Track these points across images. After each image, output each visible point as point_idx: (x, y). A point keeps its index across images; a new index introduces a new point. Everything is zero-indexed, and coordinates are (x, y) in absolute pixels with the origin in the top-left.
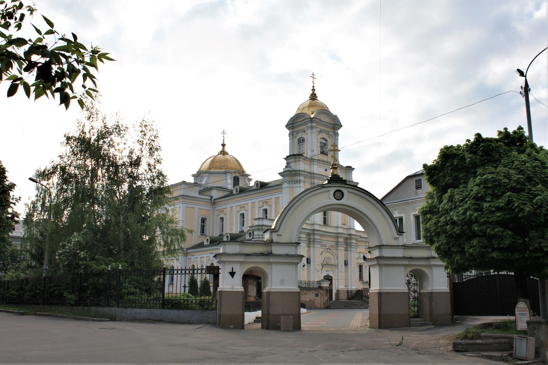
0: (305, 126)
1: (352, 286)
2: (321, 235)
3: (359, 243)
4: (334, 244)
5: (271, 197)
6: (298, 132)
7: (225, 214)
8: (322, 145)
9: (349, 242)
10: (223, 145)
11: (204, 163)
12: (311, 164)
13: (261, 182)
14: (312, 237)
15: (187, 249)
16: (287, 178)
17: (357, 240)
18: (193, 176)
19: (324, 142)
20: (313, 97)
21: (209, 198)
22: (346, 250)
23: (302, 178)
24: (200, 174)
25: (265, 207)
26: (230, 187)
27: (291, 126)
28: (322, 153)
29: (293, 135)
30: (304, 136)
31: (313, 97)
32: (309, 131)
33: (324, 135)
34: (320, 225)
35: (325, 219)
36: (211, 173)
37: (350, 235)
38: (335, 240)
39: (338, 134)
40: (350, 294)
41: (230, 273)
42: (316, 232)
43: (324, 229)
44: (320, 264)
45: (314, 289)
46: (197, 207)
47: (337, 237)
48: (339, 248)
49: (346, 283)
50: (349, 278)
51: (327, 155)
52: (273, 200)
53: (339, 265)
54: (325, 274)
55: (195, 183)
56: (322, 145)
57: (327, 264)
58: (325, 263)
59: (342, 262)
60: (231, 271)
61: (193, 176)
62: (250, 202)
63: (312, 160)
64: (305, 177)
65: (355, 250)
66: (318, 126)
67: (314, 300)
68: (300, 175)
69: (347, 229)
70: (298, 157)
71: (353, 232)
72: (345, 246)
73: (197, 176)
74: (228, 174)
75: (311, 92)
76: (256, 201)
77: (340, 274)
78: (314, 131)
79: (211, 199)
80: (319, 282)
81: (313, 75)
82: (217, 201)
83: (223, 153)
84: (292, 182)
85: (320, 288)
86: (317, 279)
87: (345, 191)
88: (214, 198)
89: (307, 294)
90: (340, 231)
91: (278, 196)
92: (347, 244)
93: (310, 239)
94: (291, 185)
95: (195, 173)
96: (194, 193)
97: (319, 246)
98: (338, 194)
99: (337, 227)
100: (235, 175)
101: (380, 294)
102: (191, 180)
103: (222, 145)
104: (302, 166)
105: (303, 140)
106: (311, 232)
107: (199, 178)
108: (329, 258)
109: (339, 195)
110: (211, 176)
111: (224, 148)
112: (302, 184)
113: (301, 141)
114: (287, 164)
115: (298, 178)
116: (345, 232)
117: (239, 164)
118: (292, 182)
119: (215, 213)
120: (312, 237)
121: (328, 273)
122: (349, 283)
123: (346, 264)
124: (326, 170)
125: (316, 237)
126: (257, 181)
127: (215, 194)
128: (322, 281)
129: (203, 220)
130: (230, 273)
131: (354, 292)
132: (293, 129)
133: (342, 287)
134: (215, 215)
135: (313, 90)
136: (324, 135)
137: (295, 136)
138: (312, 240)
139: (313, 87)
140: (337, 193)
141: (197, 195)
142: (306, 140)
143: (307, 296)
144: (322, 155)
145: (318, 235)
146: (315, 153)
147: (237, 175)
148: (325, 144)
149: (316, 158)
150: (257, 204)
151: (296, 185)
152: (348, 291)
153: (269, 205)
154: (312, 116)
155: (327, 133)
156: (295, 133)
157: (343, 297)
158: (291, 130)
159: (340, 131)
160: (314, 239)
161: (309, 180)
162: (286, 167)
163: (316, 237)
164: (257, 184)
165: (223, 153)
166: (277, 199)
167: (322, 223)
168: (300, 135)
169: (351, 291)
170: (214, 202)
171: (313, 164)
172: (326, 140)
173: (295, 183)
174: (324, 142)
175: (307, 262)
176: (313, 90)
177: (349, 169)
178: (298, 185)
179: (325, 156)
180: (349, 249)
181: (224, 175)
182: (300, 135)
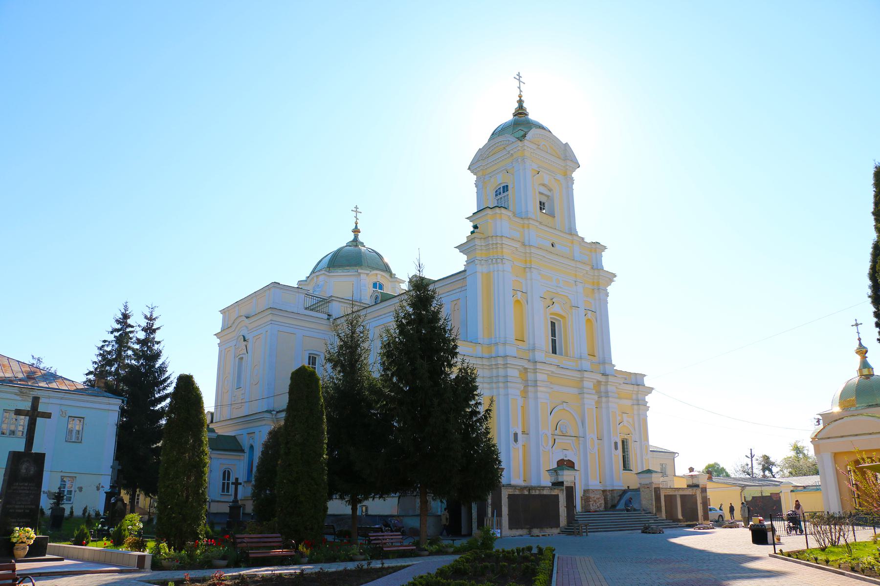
10: (356, 231)
11: (320, 261)
14: (531, 376)
35: (554, 342)
40: (609, 497)
43: (554, 359)
58: (557, 432)
75: (516, 105)
79: (328, 319)
82: (338, 322)
83: (356, 242)
92: (598, 392)
100: (375, 280)
105: (506, 188)
114: (475, 227)
120: (531, 376)
133: (595, 484)
135: (520, 102)
138: (530, 383)
157: (598, 503)
159: (575, 175)
162: (472, 233)
165: (356, 242)
168: (500, 179)
176: (520, 102)
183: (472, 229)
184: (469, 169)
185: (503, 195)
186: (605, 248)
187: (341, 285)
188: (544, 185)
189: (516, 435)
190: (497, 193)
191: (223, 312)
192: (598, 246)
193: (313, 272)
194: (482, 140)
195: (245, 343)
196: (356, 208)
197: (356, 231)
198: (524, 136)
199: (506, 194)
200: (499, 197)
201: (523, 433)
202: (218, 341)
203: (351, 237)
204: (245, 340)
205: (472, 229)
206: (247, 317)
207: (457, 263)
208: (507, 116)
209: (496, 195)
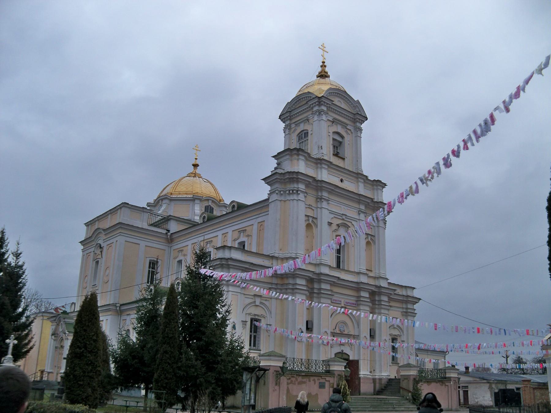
0: (310, 112)
1: (381, 372)
2: (333, 284)
3: (392, 304)
4: (352, 300)
5: (252, 223)
6: (297, 124)
7: (185, 255)
8: (337, 144)
9: (377, 298)
10: (196, 166)
12: (317, 168)
13: (237, 202)
14: (316, 286)
15: (121, 305)
16: (277, 185)
17: (390, 299)
19: (339, 139)
20: (323, 75)
21: (165, 232)
23: (302, 187)
24: (158, 202)
25: (242, 239)
26: (197, 219)
27: (288, 115)
28: (336, 155)
29: (290, 129)
30: (307, 127)
31: (323, 75)
32: (316, 118)
33: (339, 129)
34: (330, 267)
35: (338, 258)
36: (171, 200)
37: (380, 287)
38: (356, 294)
39: (361, 130)
44: (329, 332)
46: (143, 244)
47: (358, 290)
48: (362, 307)
49: (371, 368)
50: (377, 359)
51: (344, 159)
52: (255, 227)
53: (362, 336)
54: (337, 350)
56: (337, 144)
57: (341, 334)
59: (365, 333)
62: (220, 234)
63: (319, 162)
64: (308, 185)
65: (386, 312)
66: (330, 113)
67: (317, 394)
68: (297, 181)
69: (375, 278)
70: (295, 152)
71: (384, 284)
72: (370, 304)
73: (155, 206)
74: (196, 201)
75: (320, 69)
76: (229, 230)
77: (362, 350)
78: (324, 117)
79: (167, 233)
80: (327, 363)
82: (174, 236)
84: (285, 192)
85: (329, 372)
86: (323, 357)
88: (171, 232)
89: (305, 383)
90: (364, 279)
91: (260, 220)
92: (373, 301)
93: (313, 289)
94: (282, 198)
95: (152, 201)
96: (142, 222)
97: (329, 302)
99: (359, 273)
100: (207, 204)
103: (193, 165)
104: (301, 166)
105: (306, 134)
107: (157, 208)
108: (344, 323)
110: (173, 203)
112: (301, 196)
113: (304, 135)
115: (296, 186)
116: (372, 282)
117: (215, 190)
118: (285, 192)
119: (172, 254)
120: (316, 286)
121: (342, 348)
122: (377, 367)
123: (372, 336)
124: (342, 181)
125: (324, 286)
126: (233, 202)
127: (174, 227)
129: (153, 264)
131: (384, 382)
132: (290, 120)
134: (172, 258)
135: (323, 66)
136: (339, 129)
137: (293, 130)
139: (323, 62)
141: (145, 226)
142: (310, 133)
143: (304, 386)
144: (336, 158)
145: (327, 282)
146: (324, 151)
147: (210, 203)
148: (340, 143)
149: (325, 158)
150: (230, 235)
151: (292, 197)
152: (374, 380)
153: (248, 236)
154: (320, 96)
155: (344, 125)
156: (293, 126)
158: (288, 122)
160: (320, 289)
161: (314, 193)
162: (276, 168)
163: (324, 286)
164: (234, 206)
166: (261, 224)
167: (334, 265)
168: (302, 127)
169: (380, 379)
170: (170, 239)
171: (321, 168)
172: (342, 137)
173: (289, 194)
174: (339, 139)
175: (308, 329)
176: (323, 66)
177: (379, 184)
178: (295, 197)
179: (340, 160)
180: (377, 311)
181: (191, 203)
182: (302, 127)
183: (276, 166)
184: (280, 118)
191: (87, 224)
202: (82, 247)
205: (276, 166)
207: (262, 192)
209: (299, 140)
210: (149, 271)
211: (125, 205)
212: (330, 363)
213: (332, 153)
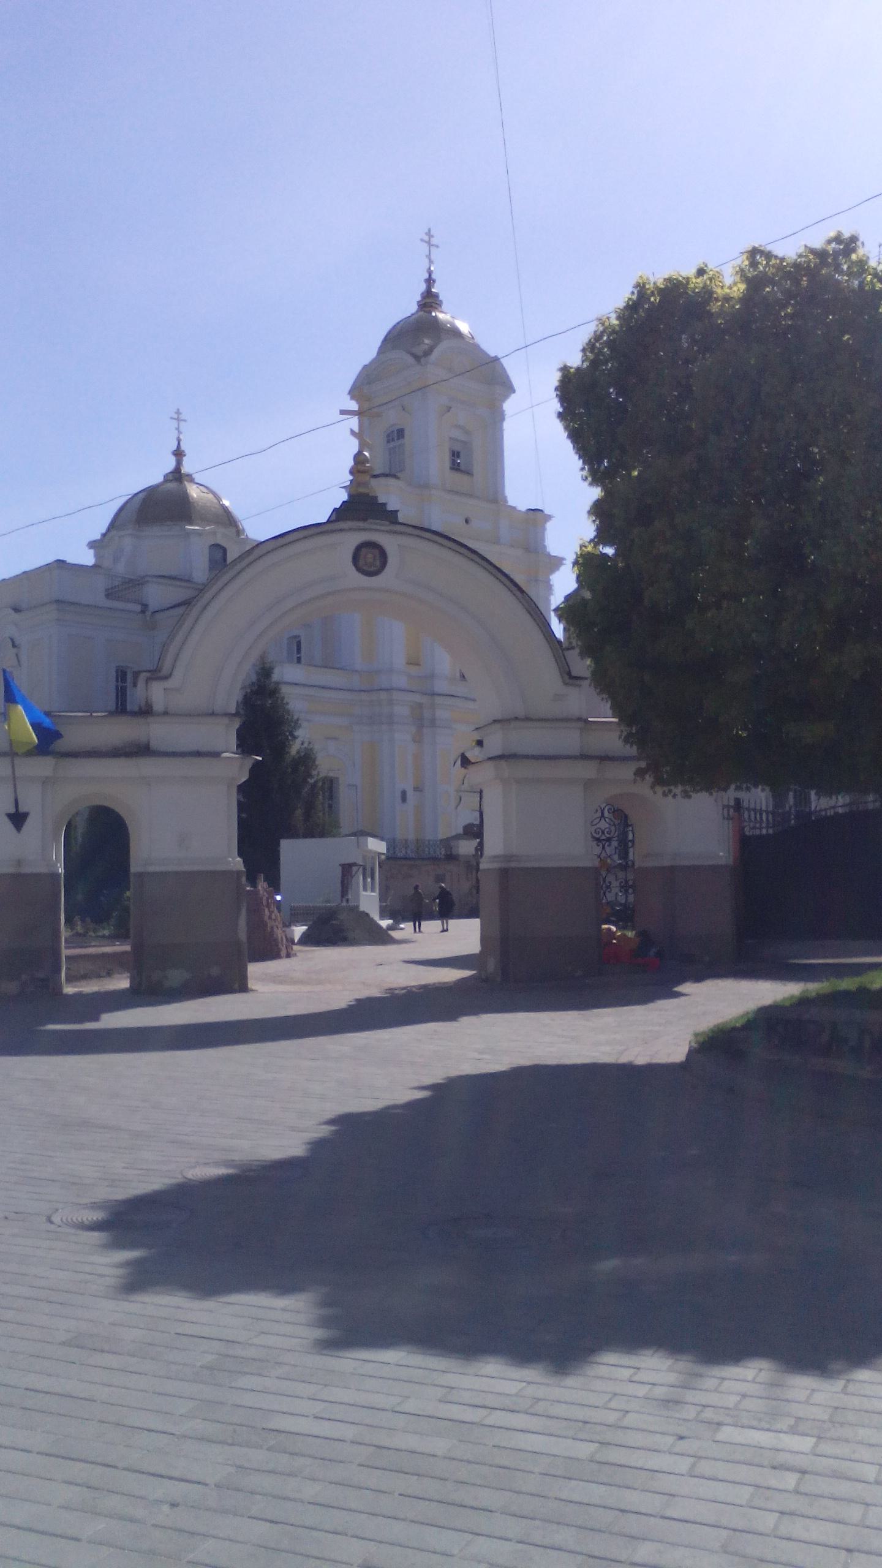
10: (179, 454)
18: (92, 545)
21: (138, 608)
22: (418, 739)
41: (9, 816)
42: (439, 700)
45: (434, 859)
55: (95, 566)
60: (12, 810)
61: (92, 545)
75: (423, 287)
79: (143, 612)
80: (447, 842)
81: (429, 233)
82: (158, 616)
83: (177, 475)
85: (451, 857)
86: (443, 833)
87: (389, 542)
88: (151, 609)
98: (369, 556)
101: (505, 874)
102: (88, 558)
105: (401, 433)
106: (424, 700)
109: (370, 560)
111: (179, 463)
124: (467, 521)
128: (457, 837)
130: (9, 816)
135: (430, 281)
140: (364, 551)
142: (407, 433)
159: (509, 406)
165: (177, 475)
168: (392, 418)
176: (430, 281)
185: (397, 443)
186: (549, 517)
187: (158, 550)
188: (458, 427)
189: (404, 795)
190: (390, 438)
192: (539, 514)
193: (112, 526)
194: (368, 350)
195: (15, 650)
196: (178, 412)
197: (179, 454)
198: (428, 353)
199: (401, 441)
200: (392, 445)
201: (417, 789)
203: (170, 464)
204: (14, 646)
206: (17, 610)
208: (407, 306)
209: (388, 442)
210: (117, 687)
211: (61, 563)
212: (452, 843)
213: (447, 464)
